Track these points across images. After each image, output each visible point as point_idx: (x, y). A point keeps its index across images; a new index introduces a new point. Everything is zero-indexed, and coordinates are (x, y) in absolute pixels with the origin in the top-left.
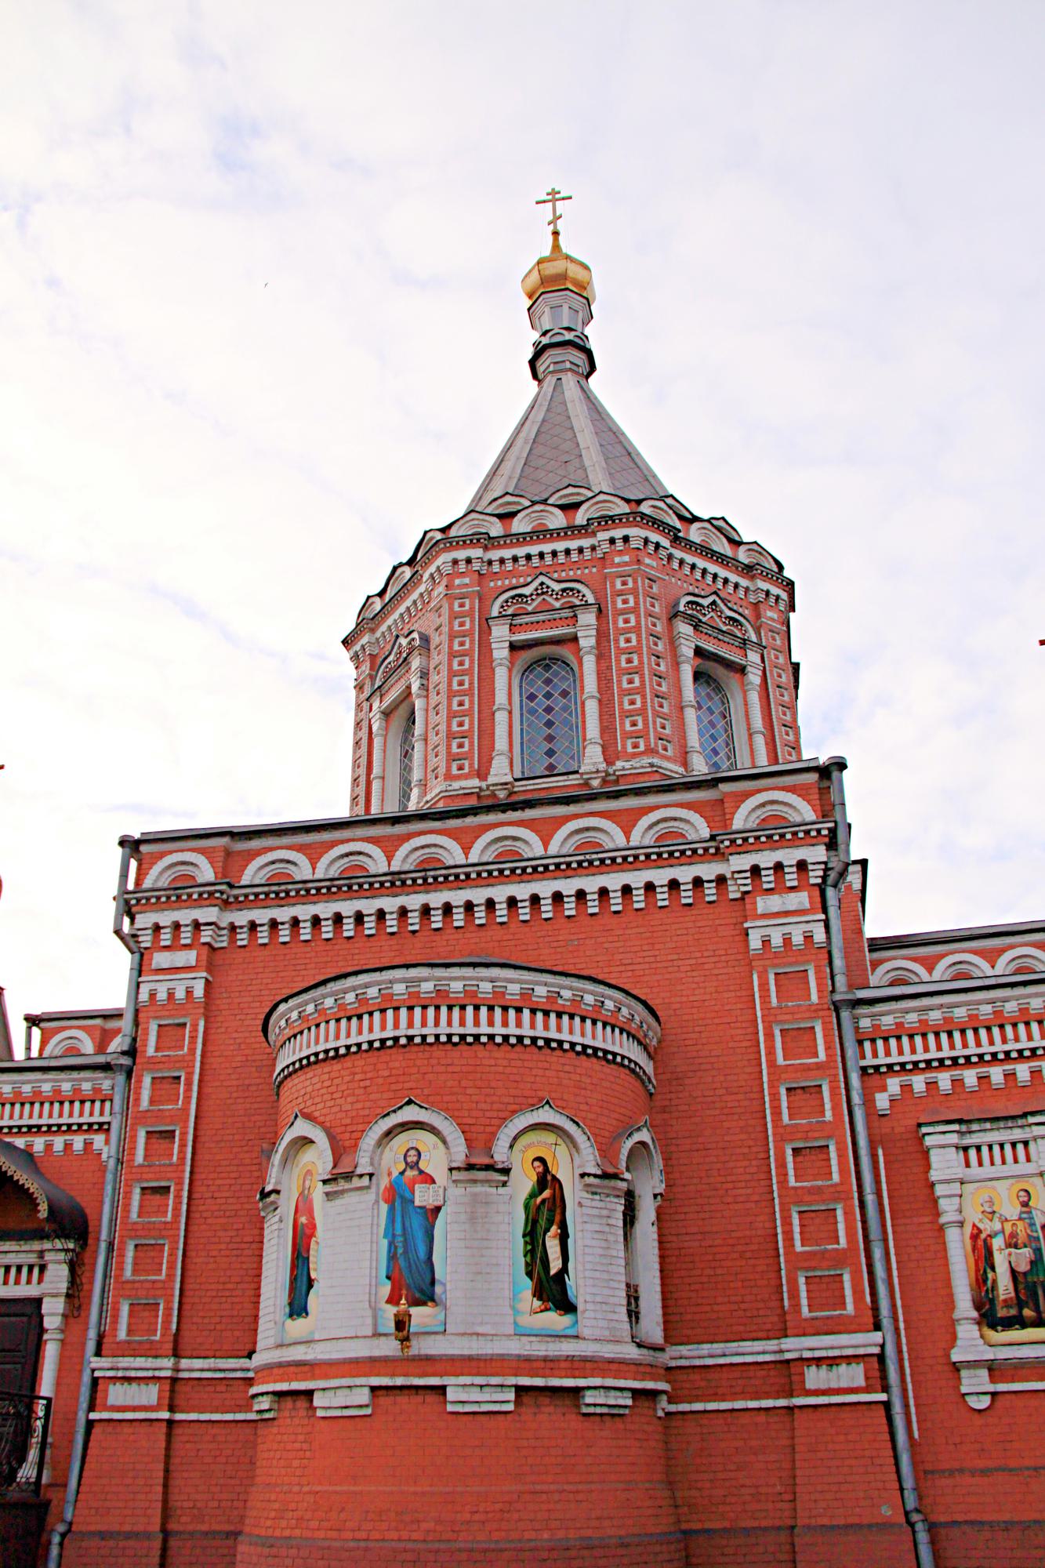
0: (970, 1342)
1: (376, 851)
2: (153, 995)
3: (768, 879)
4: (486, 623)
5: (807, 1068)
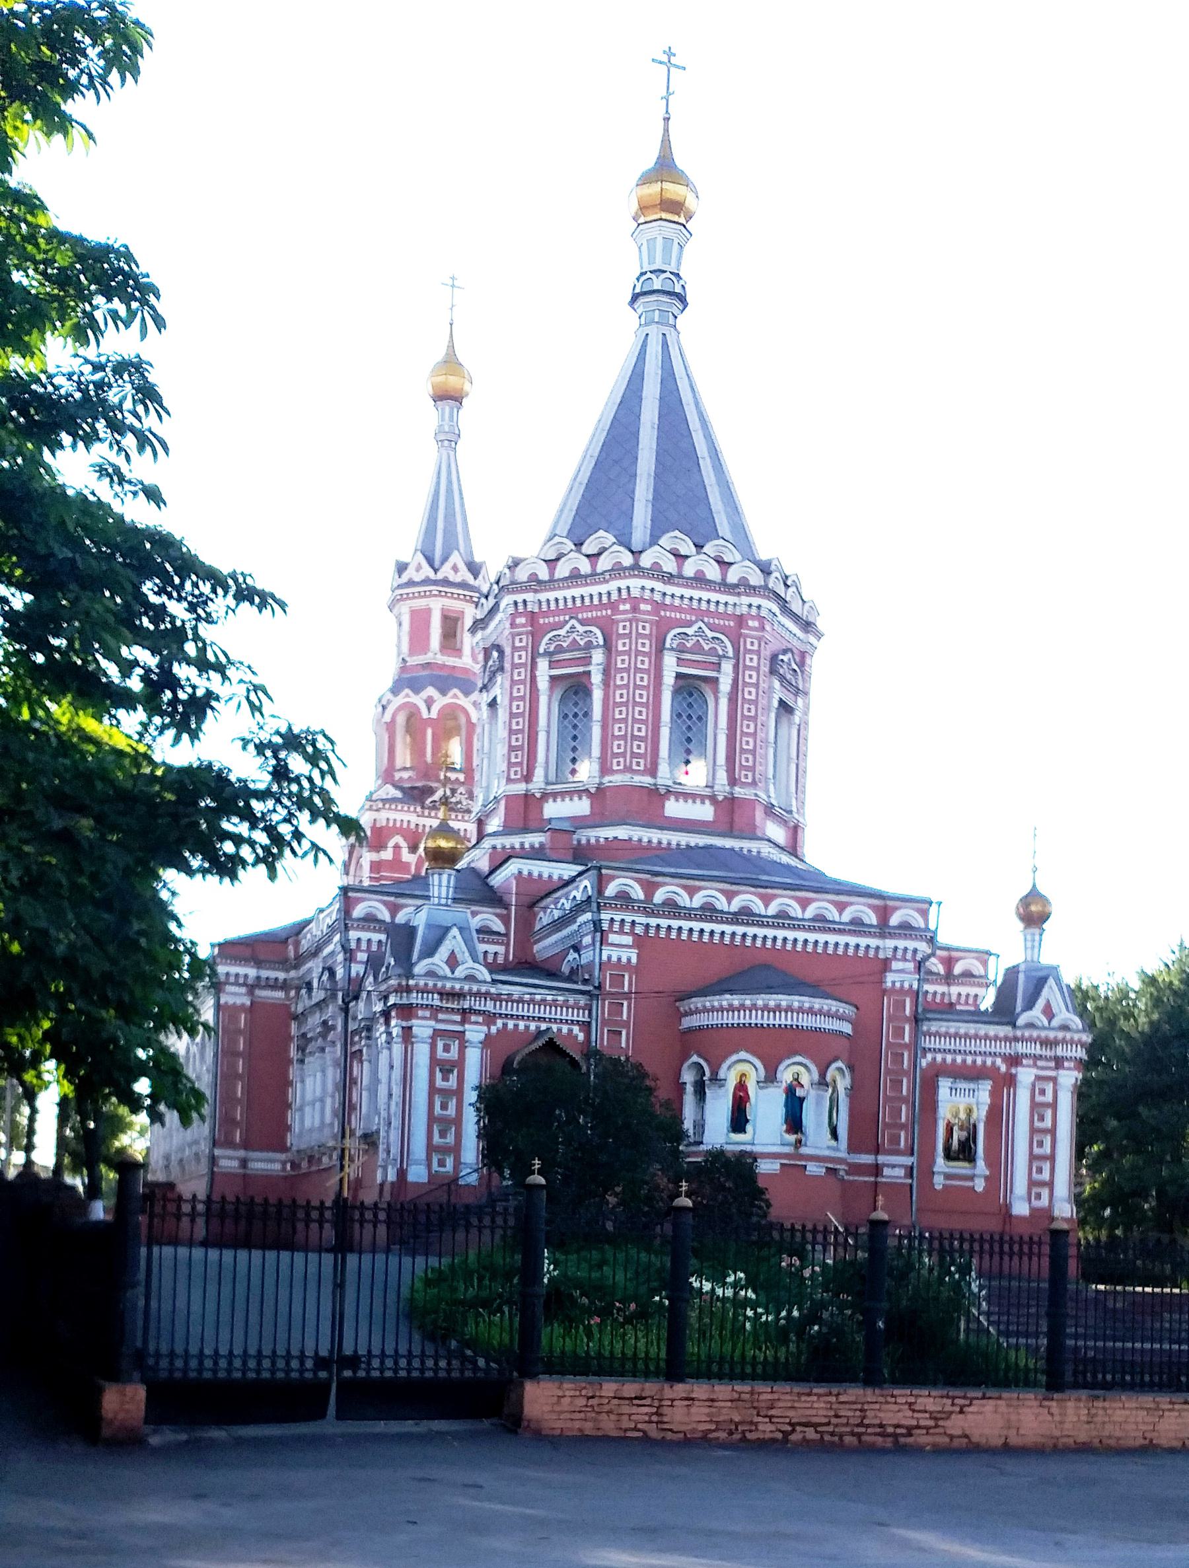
0: (940, 1163)
1: (723, 899)
2: (609, 958)
3: (900, 954)
4: (660, 649)
5: (901, 1045)
